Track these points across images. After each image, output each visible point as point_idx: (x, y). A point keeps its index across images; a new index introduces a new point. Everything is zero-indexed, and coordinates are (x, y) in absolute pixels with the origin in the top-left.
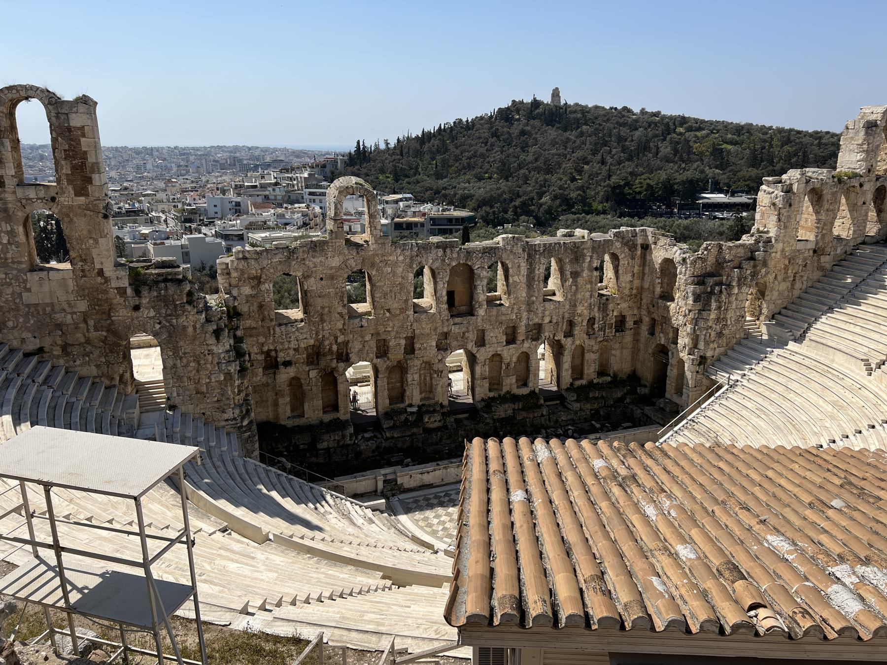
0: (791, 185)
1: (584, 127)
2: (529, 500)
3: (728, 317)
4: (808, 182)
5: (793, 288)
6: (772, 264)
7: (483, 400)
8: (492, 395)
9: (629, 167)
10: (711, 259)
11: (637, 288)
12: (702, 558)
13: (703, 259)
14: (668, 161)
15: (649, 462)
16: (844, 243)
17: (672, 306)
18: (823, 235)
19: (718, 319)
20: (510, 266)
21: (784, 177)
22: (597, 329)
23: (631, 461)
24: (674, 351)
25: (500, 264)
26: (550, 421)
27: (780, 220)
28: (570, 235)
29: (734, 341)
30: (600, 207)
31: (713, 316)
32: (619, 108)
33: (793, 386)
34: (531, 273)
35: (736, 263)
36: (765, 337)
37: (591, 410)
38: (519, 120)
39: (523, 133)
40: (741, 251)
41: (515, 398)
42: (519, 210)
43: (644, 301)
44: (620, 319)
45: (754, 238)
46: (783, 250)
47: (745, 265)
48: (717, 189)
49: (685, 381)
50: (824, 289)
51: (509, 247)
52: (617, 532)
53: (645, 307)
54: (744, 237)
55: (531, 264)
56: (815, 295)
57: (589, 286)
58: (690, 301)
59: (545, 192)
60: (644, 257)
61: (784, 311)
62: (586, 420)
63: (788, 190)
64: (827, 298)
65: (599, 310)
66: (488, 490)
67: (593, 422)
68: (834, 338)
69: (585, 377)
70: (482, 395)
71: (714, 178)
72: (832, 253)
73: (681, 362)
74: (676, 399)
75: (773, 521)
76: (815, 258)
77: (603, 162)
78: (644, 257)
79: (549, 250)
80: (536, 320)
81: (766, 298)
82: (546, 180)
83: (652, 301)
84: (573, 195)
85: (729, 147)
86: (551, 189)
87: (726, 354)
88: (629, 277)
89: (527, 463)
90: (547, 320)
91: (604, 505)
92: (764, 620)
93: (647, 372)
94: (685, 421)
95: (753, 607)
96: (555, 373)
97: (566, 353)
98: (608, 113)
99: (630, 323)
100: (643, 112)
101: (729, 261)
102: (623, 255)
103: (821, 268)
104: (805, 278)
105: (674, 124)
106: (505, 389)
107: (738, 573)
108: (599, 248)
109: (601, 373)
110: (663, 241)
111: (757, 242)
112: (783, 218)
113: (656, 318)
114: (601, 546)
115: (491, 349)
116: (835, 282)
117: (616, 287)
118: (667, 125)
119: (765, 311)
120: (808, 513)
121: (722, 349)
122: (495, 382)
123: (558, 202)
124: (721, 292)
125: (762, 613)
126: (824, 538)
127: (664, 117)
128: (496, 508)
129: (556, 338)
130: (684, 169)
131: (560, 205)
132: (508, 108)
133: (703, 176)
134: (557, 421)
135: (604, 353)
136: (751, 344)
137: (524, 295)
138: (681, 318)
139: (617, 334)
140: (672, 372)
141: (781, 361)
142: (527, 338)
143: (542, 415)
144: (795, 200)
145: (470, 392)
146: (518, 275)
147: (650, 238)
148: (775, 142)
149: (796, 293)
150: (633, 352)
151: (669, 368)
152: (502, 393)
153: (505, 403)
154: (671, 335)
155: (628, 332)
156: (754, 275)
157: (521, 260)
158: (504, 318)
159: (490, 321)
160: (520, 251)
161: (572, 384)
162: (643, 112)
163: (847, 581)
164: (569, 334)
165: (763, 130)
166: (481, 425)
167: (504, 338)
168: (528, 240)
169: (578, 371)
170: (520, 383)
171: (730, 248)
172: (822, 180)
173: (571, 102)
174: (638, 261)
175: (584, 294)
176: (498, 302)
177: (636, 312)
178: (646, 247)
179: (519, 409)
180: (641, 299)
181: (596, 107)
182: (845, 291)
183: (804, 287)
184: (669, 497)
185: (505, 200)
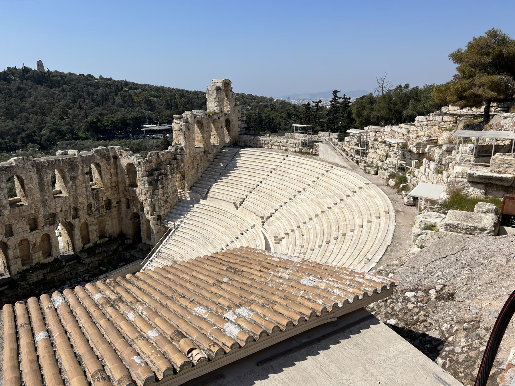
0: (188, 119)
1: (64, 86)
2: (50, 336)
3: (169, 191)
4: (195, 117)
5: (198, 172)
6: (185, 161)
7: (18, 273)
8: (25, 268)
9: (98, 110)
10: (154, 161)
11: (115, 182)
12: (162, 334)
13: (150, 162)
14: (121, 106)
15: (129, 286)
17: (137, 190)
19: (163, 193)
20: (24, 178)
21: (183, 115)
22: (94, 211)
23: (118, 289)
24: (143, 215)
25: (16, 178)
26: (71, 274)
28: (66, 154)
29: (174, 204)
30: (84, 135)
31: (160, 192)
32: (86, 75)
33: (206, 222)
34: (41, 180)
35: (168, 162)
36: (189, 199)
37: (98, 261)
38: (15, 80)
39: (19, 89)
40: (169, 156)
41: (43, 266)
42: (26, 140)
43: (120, 189)
44: (108, 202)
46: (190, 153)
47: (172, 162)
48: (151, 122)
50: (212, 171)
51: (21, 165)
52: (112, 337)
53: (121, 192)
54: (169, 148)
55: (40, 175)
57: (84, 185)
58: (147, 186)
59: (44, 127)
61: (195, 185)
62: (96, 268)
63: (187, 122)
65: (93, 198)
66: (17, 340)
67: (101, 268)
68: (220, 195)
69: (91, 241)
70: (18, 270)
71: (149, 116)
73: (148, 221)
74: (148, 242)
75: (197, 299)
77: (81, 108)
79: (52, 165)
80: (51, 211)
81: (186, 179)
82: (42, 120)
83: (125, 189)
84: (64, 128)
85: (154, 99)
86: (48, 125)
87: (171, 212)
88: (108, 176)
89: (47, 311)
90: (59, 210)
91: (102, 323)
92: (196, 356)
93: (129, 231)
94: (155, 253)
95: (190, 351)
96: (70, 243)
97: (76, 229)
98: (79, 78)
99: (114, 204)
100: (101, 77)
101: (164, 161)
102: (103, 164)
103: (208, 161)
104: (202, 166)
105: (121, 85)
106: (35, 262)
107: (180, 335)
108: (87, 161)
109: (101, 237)
110: (125, 153)
112: (187, 137)
113: (129, 198)
114: (101, 350)
115: (19, 237)
117: (102, 183)
119: (186, 186)
120: (213, 289)
121: (168, 210)
122: (26, 259)
123: (54, 133)
124: (162, 178)
125: (194, 352)
126: (221, 300)
127: (114, 81)
128: (24, 350)
129: (67, 221)
130: (131, 111)
131: (56, 135)
132: (5, 72)
133: (142, 115)
134: (77, 273)
135: (101, 224)
136: (182, 204)
137: (39, 196)
138: (143, 196)
139: (107, 211)
140: (143, 228)
141: (198, 210)
142: (46, 224)
143: (66, 272)
144: (191, 127)
145: (7, 270)
146: (32, 184)
147: (117, 152)
148: (177, 97)
149: (200, 174)
150: (119, 220)
151: (141, 225)
152: (33, 265)
153: (36, 271)
154: (139, 207)
155: (114, 209)
156: (178, 167)
157: (32, 173)
158: (25, 214)
159: (14, 217)
160: (30, 167)
161: (83, 248)
162: (101, 77)
163: (232, 319)
164: (76, 216)
165: (170, 90)
166: (20, 290)
167: (28, 227)
168: (35, 159)
169: (86, 239)
170: (46, 255)
171: (163, 154)
173: (52, 70)
174: (112, 166)
175: (82, 190)
176: (19, 204)
177: (116, 196)
178: (116, 158)
179: (47, 273)
180: (119, 189)
181: (70, 74)
182: (221, 171)
184: (142, 303)
185: (13, 134)
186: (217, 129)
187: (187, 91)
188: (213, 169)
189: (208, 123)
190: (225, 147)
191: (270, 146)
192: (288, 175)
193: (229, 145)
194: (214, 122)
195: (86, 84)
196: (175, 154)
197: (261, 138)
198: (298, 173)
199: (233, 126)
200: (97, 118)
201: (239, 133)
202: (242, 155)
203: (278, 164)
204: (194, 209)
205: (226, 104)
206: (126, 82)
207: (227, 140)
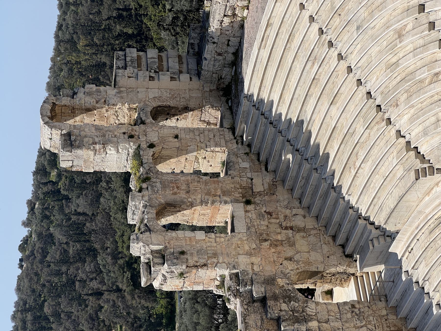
1: (46, 309)
4: (148, 229)
16: (233, 159)
18: (225, 193)
27: (205, 265)
32: (20, 255)
45: (232, 299)
46: (249, 254)
47: (274, 313)
72: (249, 175)
76: (257, 199)
77: (98, 294)
100: (26, 224)
103: (271, 190)
104: (288, 212)
105: (45, 184)
112: (202, 261)
116: (292, 174)
118: (46, 194)
119: (340, 269)
127: (35, 193)
148: (73, 58)
149: (310, 223)
156: (288, 297)
162: (26, 224)
172: (145, 206)
181: (19, 289)
182: (306, 166)
183: (301, 212)
186: (181, 151)
187: (60, 27)
189: (164, 186)
190: (233, 129)
193: (228, 114)
194: (159, 159)
195: (42, 262)
196: (250, 301)
197: (214, 25)
199: (173, 97)
200: (121, 267)
201: (195, 79)
202: (265, 96)
203: (306, 14)
204: (418, 275)
205: (111, 112)
206: (35, 173)
207: (213, 115)
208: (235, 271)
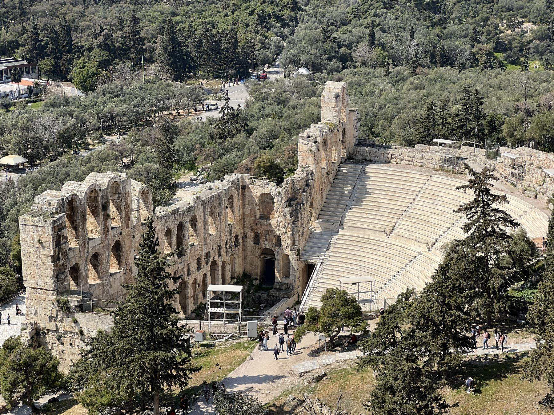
6: (315, 185)
7: (192, 312)
8: (195, 307)
24: (279, 250)
49: (291, 267)
50: (336, 195)
53: (248, 226)
56: (333, 199)
60: (243, 194)
61: (322, 212)
64: (341, 200)
74: (285, 281)
78: (243, 194)
80: (208, 250)
81: (314, 206)
101: (300, 189)
110: (258, 182)
111: (308, 175)
112: (317, 158)
113: (260, 232)
124: (301, 208)
151: (276, 262)
164: (219, 255)
174: (241, 197)
180: (244, 222)
188: (337, 193)
190: (341, 163)
191: (399, 160)
192: (439, 199)
198: (451, 197)
201: (354, 144)
208: (314, 172)
